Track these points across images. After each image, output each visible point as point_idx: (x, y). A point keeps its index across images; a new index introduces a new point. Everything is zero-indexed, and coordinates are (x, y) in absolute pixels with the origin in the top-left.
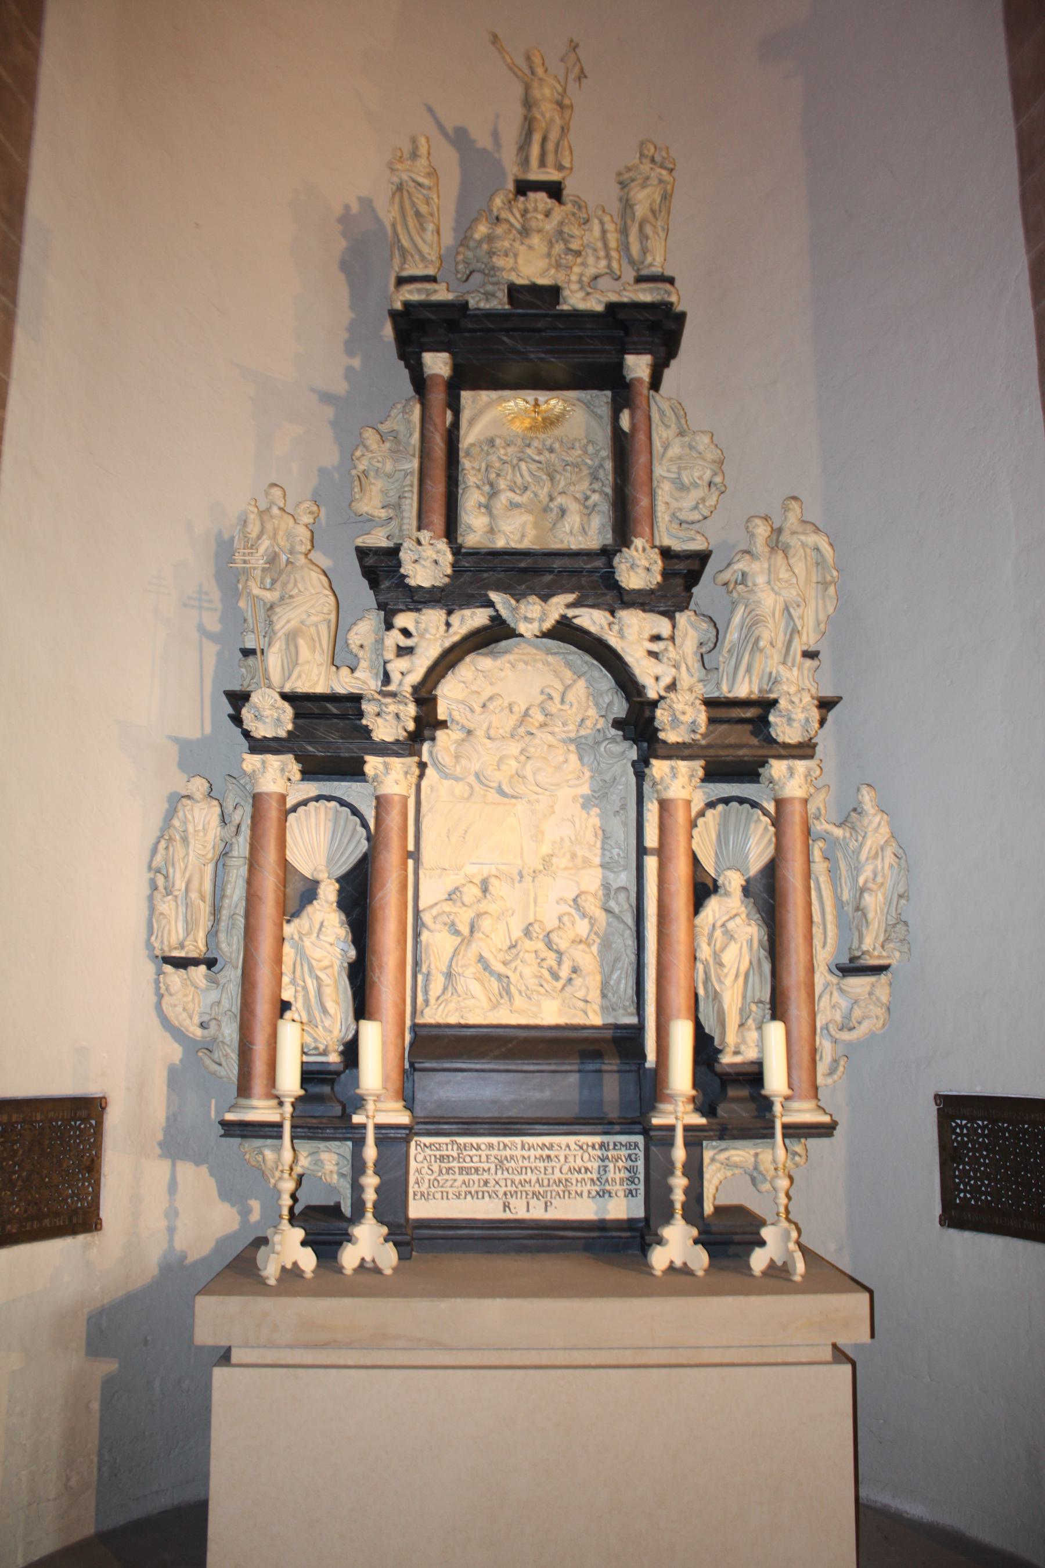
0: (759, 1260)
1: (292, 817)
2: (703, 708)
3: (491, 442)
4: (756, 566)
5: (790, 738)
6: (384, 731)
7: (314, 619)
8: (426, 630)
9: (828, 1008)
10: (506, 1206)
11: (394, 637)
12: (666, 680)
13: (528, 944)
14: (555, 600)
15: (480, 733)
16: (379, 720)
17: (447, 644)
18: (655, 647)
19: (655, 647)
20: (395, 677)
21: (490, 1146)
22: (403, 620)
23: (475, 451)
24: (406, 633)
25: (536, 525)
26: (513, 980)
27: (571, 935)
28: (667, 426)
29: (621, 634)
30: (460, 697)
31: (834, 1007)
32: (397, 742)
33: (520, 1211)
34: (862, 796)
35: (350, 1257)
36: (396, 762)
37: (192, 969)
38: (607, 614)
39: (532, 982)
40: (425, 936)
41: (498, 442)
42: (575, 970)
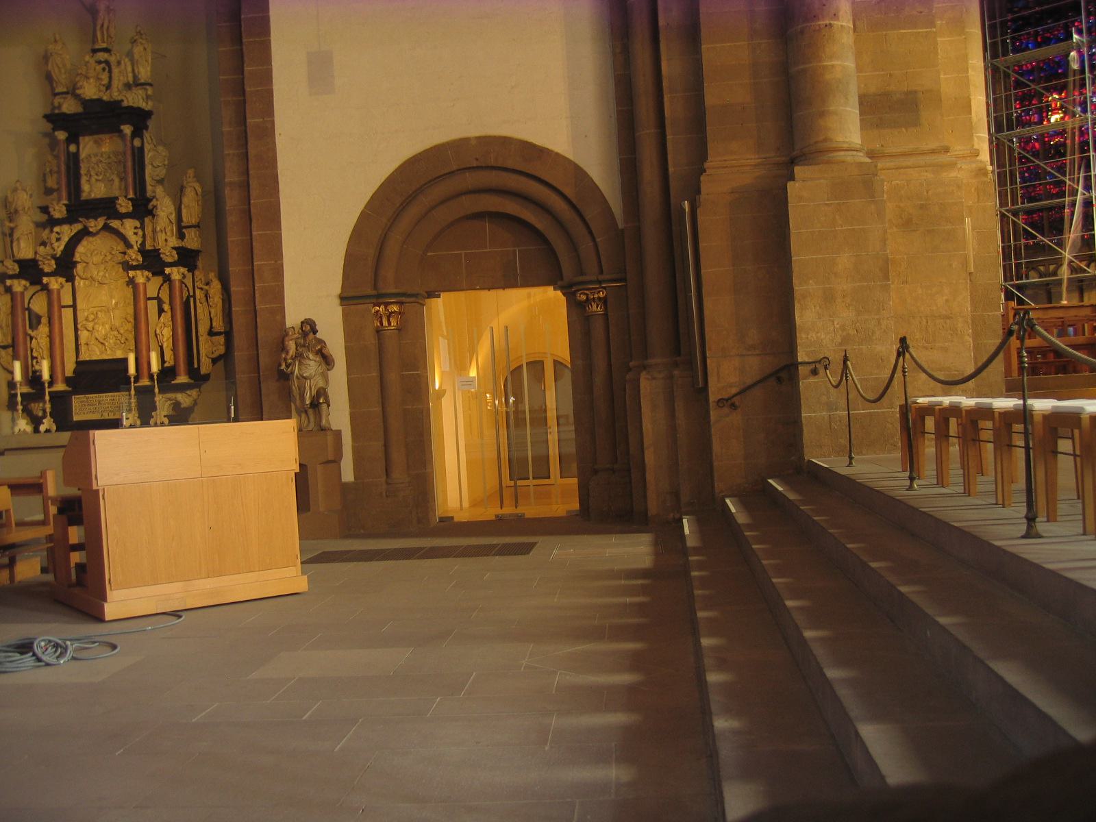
0: (152, 422)
1: (34, 297)
2: (139, 254)
3: (90, 156)
4: (159, 203)
6: (47, 270)
7: (25, 233)
8: (63, 233)
10: (102, 415)
11: (54, 236)
12: (139, 242)
13: (112, 333)
14: (99, 219)
15: (91, 263)
16: (45, 266)
17: (70, 236)
18: (136, 231)
19: (136, 231)
20: (56, 248)
21: (96, 397)
22: (56, 229)
23: (85, 161)
24: (57, 233)
25: (105, 187)
26: (107, 344)
27: (126, 328)
28: (149, 144)
29: (125, 228)
30: (84, 251)
32: (52, 272)
33: (106, 417)
35: (42, 428)
36: (52, 279)
37: (8, 349)
38: (120, 221)
39: (113, 345)
40: (79, 332)
41: (92, 156)
42: (126, 339)
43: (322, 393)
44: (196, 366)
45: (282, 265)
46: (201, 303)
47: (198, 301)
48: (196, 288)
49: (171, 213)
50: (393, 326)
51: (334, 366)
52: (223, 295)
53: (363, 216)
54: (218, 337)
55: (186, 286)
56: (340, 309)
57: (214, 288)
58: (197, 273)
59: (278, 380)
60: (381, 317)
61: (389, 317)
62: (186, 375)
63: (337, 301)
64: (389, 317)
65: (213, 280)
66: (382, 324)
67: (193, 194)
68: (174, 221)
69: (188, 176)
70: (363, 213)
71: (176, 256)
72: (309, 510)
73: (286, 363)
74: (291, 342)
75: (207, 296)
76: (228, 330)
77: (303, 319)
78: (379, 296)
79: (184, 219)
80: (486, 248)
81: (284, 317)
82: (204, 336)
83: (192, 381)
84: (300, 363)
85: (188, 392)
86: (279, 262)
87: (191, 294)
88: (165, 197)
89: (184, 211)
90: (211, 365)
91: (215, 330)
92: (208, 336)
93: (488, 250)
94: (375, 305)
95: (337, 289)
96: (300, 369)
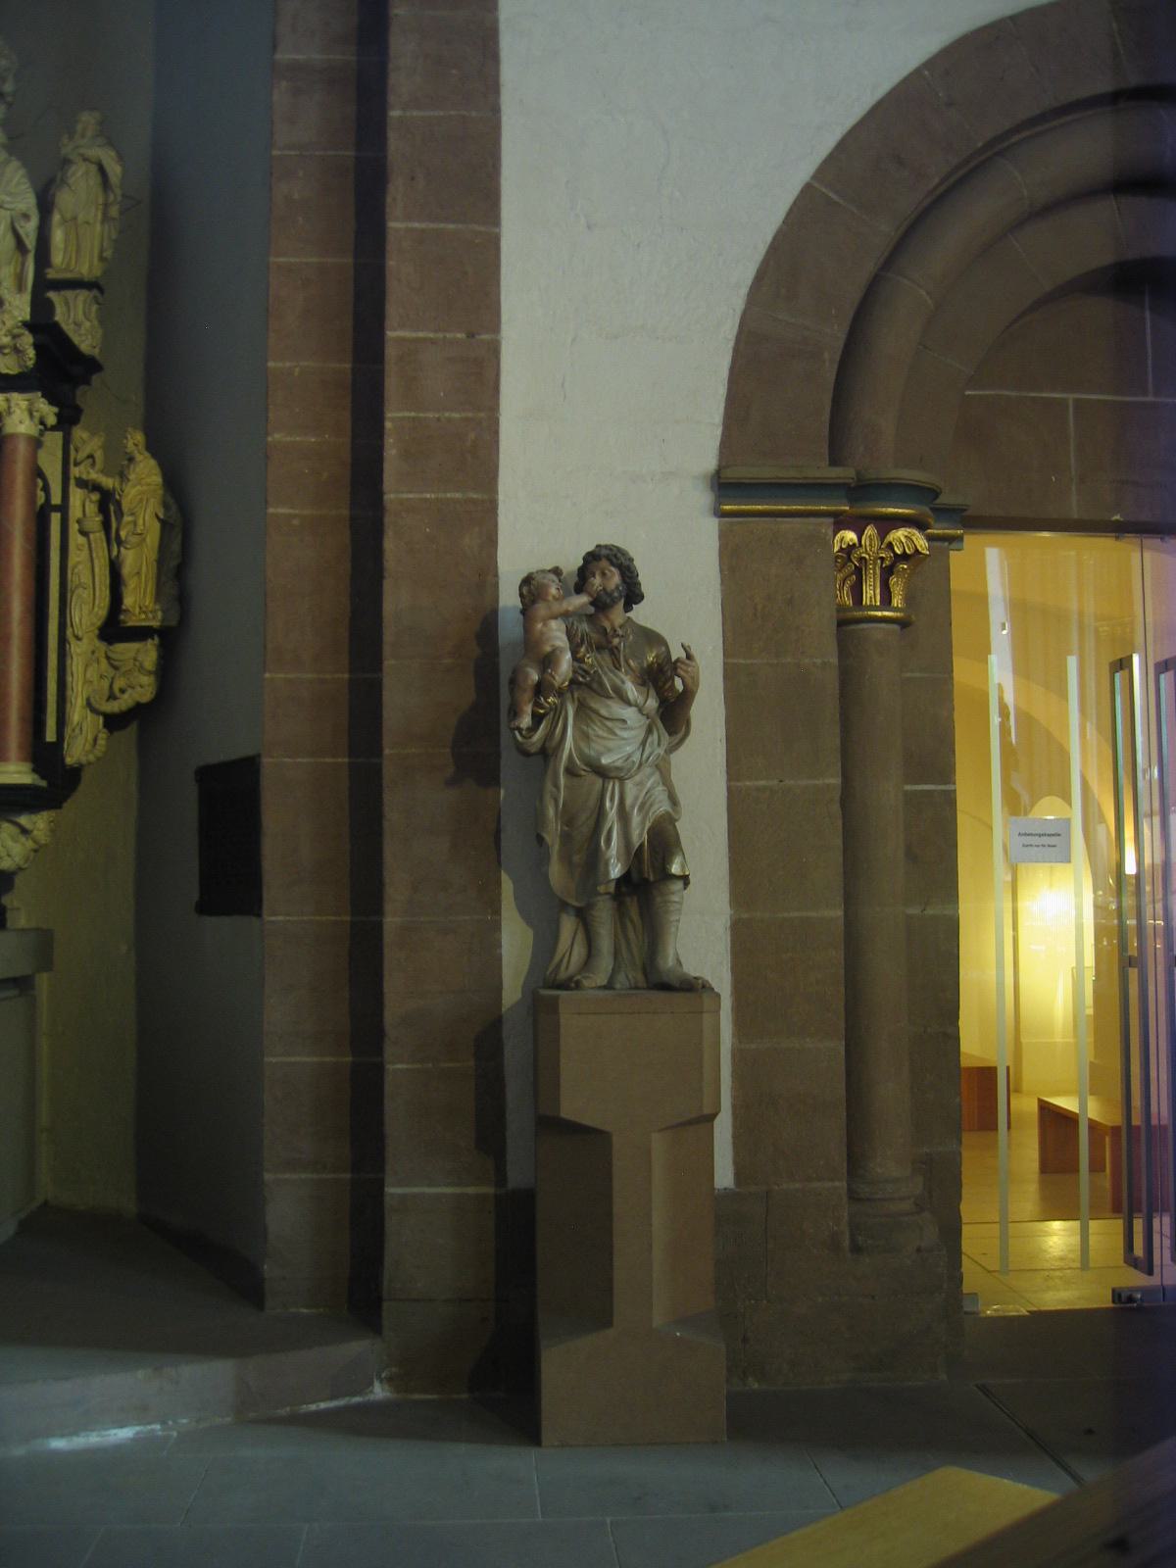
5: (8, 368)
9: (95, 678)
31: (101, 677)
34: (127, 438)
43: (662, 842)
44: (50, 736)
45: (494, 350)
46: (84, 533)
47: (74, 527)
48: (72, 482)
49: (26, 217)
50: (896, 610)
51: (687, 733)
52: (166, 506)
53: (808, 210)
54: (133, 646)
55: (38, 473)
56: (711, 526)
57: (139, 482)
58: (79, 433)
59: (451, 783)
60: (858, 571)
61: (887, 572)
62: (25, 760)
63: (703, 498)
64: (887, 572)
65: (139, 457)
66: (857, 592)
67: (94, 180)
68: (30, 242)
69: (79, 127)
70: (807, 190)
71: (31, 353)
72: (604, 1320)
73: (537, 704)
74: (553, 624)
75: (108, 503)
76: (174, 623)
77: (591, 548)
78: (863, 489)
79: (57, 258)
80: (1145, 393)
81: (491, 541)
82: (85, 641)
83: (43, 783)
84: (583, 710)
85: (24, 820)
86: (485, 337)
87: (56, 500)
88: (7, 162)
89: (58, 236)
90: (103, 735)
91: (132, 621)
92: (98, 643)
93: (1150, 398)
94: (841, 522)
95: (705, 455)
96: (583, 736)
